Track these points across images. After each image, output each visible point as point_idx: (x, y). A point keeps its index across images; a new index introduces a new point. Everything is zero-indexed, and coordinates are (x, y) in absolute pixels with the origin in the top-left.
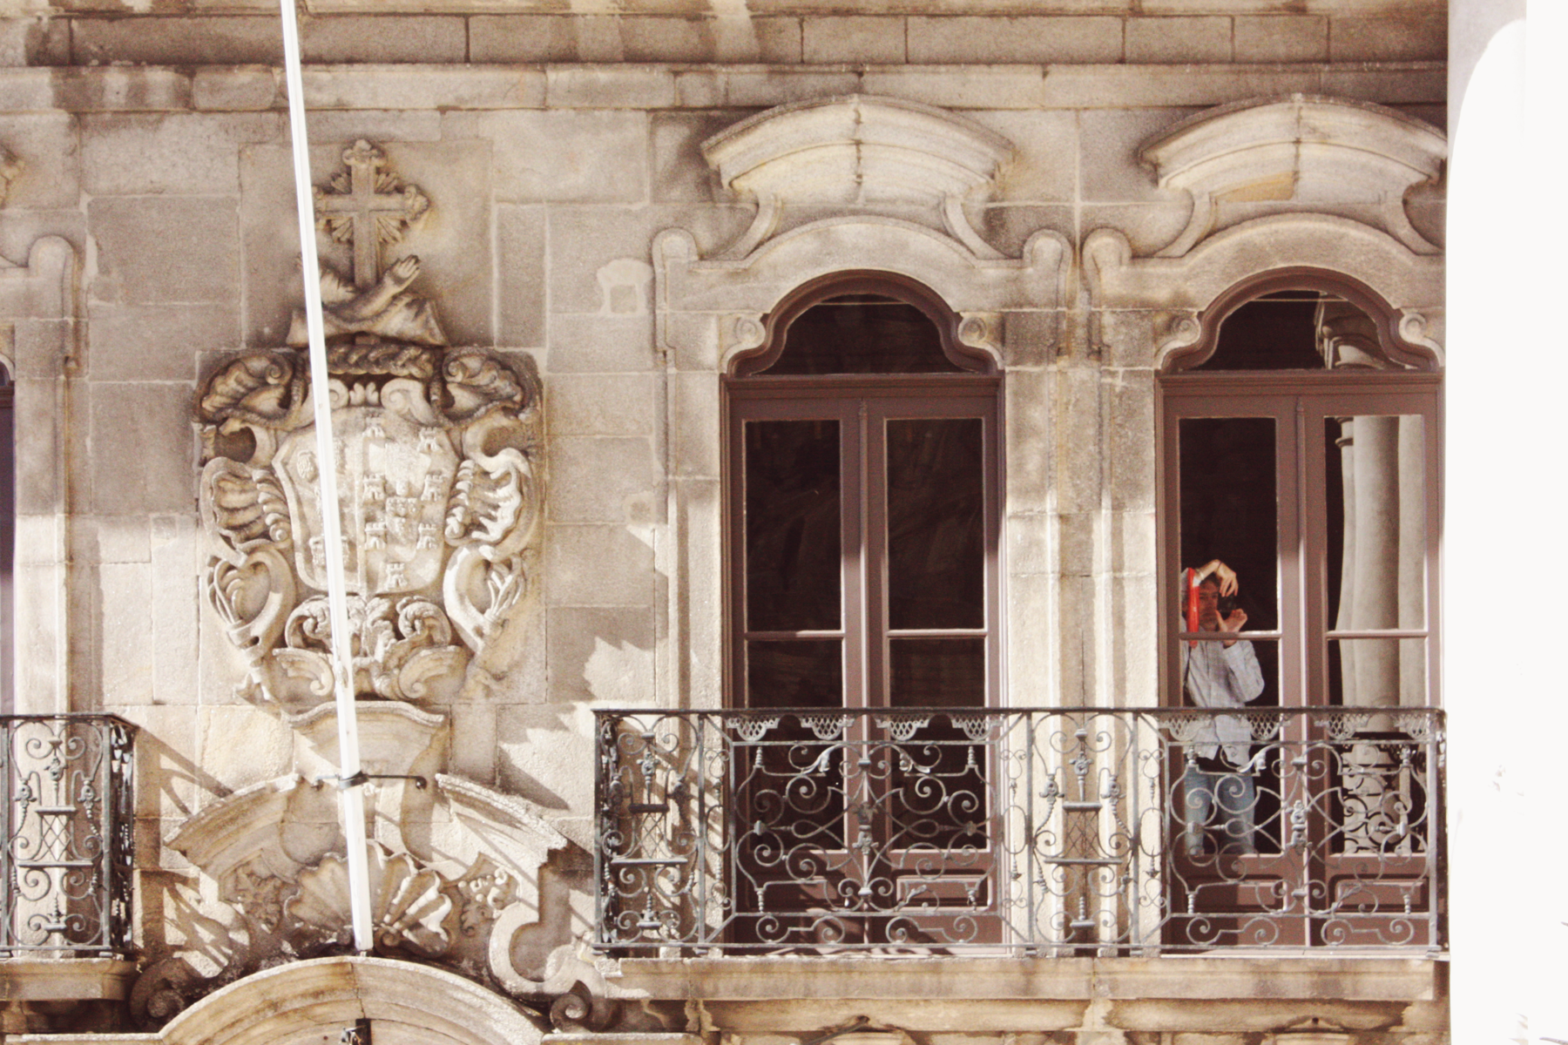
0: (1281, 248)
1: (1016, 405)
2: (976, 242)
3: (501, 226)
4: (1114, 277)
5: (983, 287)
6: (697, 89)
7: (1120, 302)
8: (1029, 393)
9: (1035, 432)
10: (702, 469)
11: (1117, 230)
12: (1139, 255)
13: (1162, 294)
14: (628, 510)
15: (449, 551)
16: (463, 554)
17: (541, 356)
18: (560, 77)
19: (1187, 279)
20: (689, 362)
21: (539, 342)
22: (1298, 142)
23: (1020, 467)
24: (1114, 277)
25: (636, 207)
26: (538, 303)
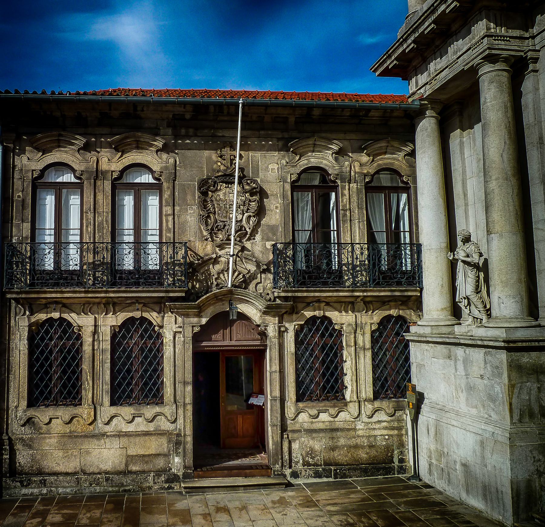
0: (385, 164)
1: (341, 190)
2: (334, 162)
3: (251, 157)
4: (357, 169)
5: (335, 170)
6: (286, 135)
7: (358, 173)
8: (343, 188)
9: (345, 195)
10: (288, 200)
11: (357, 161)
12: (361, 165)
13: (365, 172)
14: (275, 208)
15: (243, 214)
16: (246, 214)
17: (259, 180)
18: (262, 132)
19: (369, 169)
20: (285, 181)
21: (258, 177)
22: (387, 146)
23: (342, 201)
24: (357, 169)
25: (275, 155)
26: (258, 171)
